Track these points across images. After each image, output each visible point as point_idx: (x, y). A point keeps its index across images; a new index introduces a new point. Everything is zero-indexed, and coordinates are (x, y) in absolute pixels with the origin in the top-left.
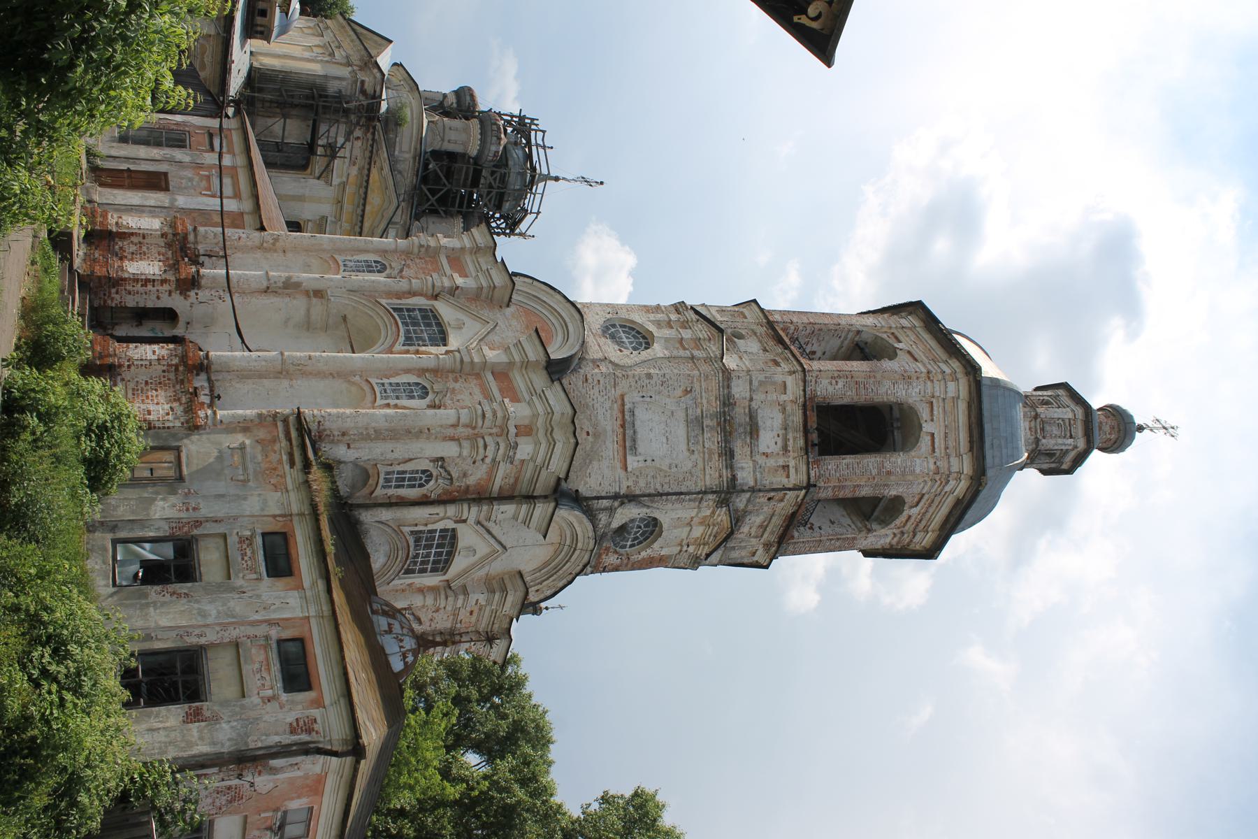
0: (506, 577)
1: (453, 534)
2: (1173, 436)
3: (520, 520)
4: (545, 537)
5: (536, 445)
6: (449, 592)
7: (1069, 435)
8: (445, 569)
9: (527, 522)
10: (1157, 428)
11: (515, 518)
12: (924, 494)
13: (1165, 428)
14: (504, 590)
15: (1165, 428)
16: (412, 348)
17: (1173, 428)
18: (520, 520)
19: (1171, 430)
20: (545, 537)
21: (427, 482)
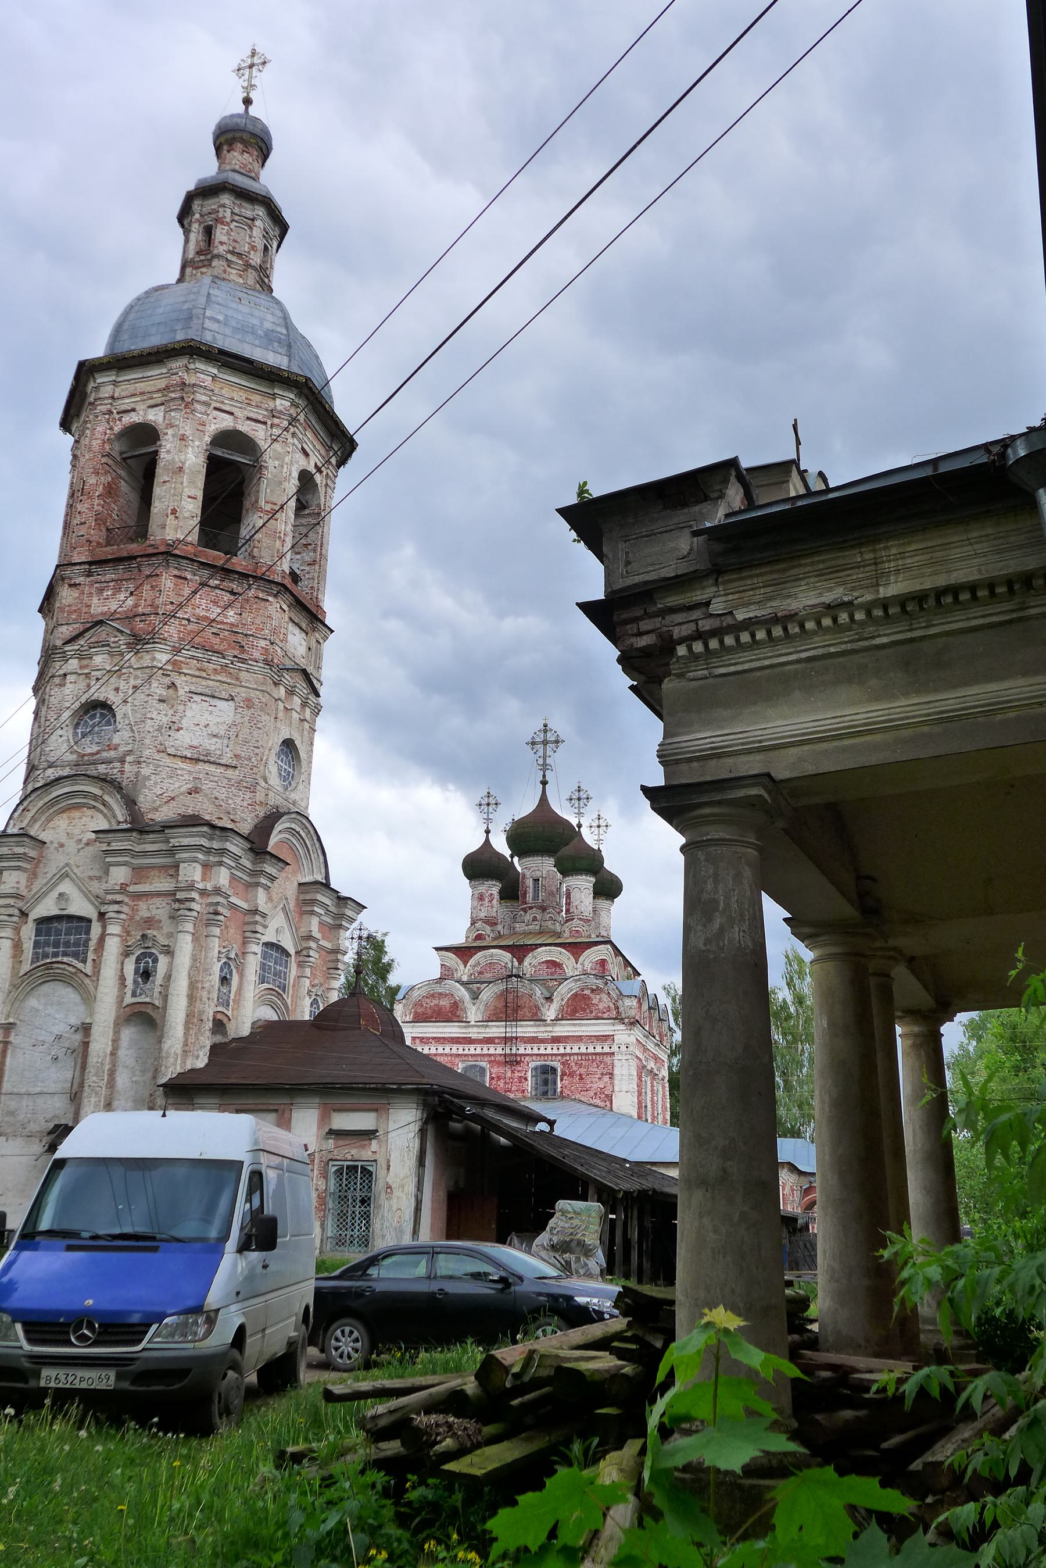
0: (302, 897)
1: (267, 944)
2: (264, 63)
3: (269, 884)
4: (289, 864)
5: (222, 865)
6: (304, 953)
7: (250, 222)
8: (288, 955)
9: (273, 879)
10: (250, 77)
11: (267, 888)
12: (303, 448)
13: (251, 66)
14: (314, 902)
15: (251, 66)
16: (91, 956)
17: (253, 54)
18: (269, 884)
19: (256, 60)
20: (289, 864)
21: (229, 966)
